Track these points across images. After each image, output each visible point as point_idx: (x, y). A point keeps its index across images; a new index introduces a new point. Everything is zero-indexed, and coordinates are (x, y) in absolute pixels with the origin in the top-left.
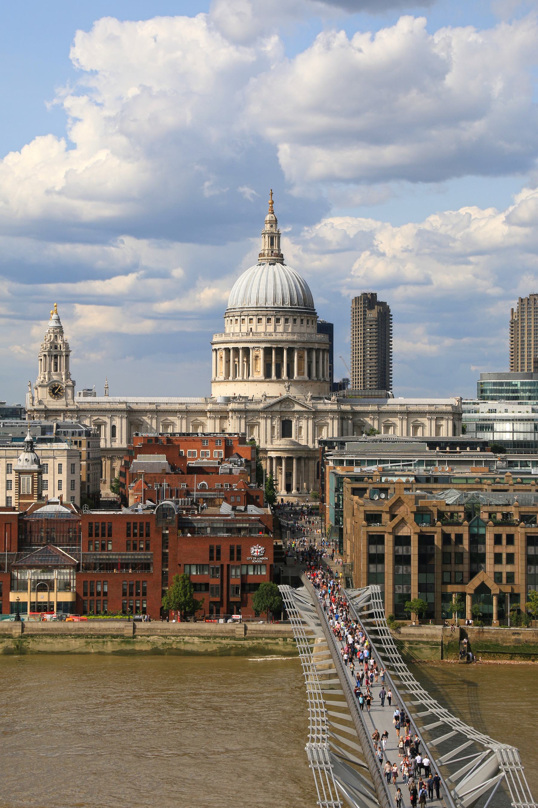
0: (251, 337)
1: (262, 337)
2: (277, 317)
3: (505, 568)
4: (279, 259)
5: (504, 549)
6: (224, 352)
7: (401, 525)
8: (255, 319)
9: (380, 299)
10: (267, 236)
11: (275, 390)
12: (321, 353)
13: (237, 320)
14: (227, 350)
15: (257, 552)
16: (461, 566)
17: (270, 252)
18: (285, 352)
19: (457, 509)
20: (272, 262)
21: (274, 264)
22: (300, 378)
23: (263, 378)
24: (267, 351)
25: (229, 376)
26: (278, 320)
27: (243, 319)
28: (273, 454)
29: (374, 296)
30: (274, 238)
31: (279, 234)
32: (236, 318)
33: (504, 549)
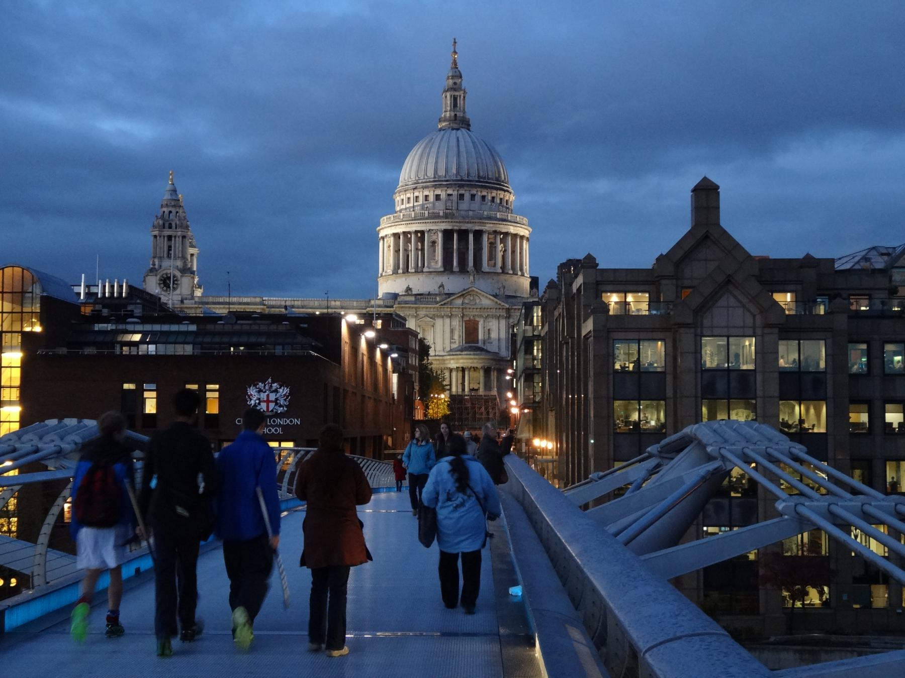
2: (460, 192)
6: (392, 238)
7: (722, 302)
10: (448, 94)
12: (518, 241)
13: (409, 198)
14: (396, 236)
15: (268, 401)
17: (453, 114)
18: (471, 237)
20: (455, 126)
21: (458, 129)
23: (442, 269)
25: (399, 268)
27: (417, 197)
31: (465, 92)
32: (408, 195)
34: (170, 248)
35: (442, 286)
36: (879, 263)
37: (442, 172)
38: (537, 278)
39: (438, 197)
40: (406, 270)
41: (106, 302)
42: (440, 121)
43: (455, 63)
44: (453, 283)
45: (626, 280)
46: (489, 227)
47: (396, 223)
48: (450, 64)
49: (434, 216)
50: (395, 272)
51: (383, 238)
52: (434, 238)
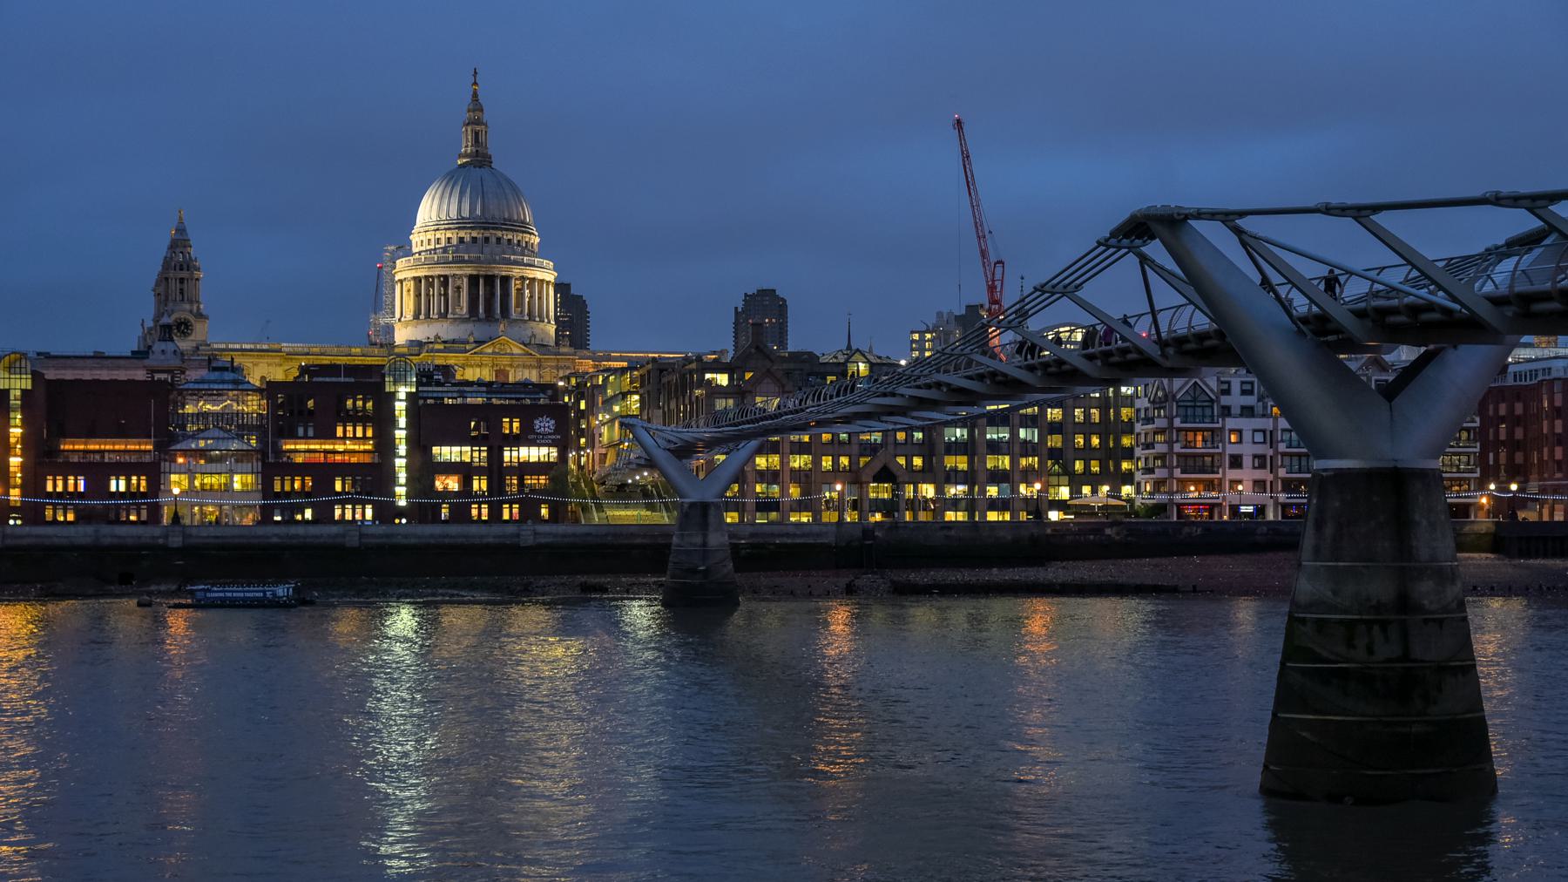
9: (573, 291)
14: (417, 280)
24: (474, 280)
29: (568, 286)
36: (841, 359)
37: (466, 214)
39: (461, 240)
40: (428, 316)
42: (461, 156)
43: (475, 94)
44: (479, 330)
45: (718, 367)
46: (516, 272)
47: (415, 267)
48: (469, 98)
49: (458, 261)
50: (416, 316)
51: (401, 281)
52: (458, 283)
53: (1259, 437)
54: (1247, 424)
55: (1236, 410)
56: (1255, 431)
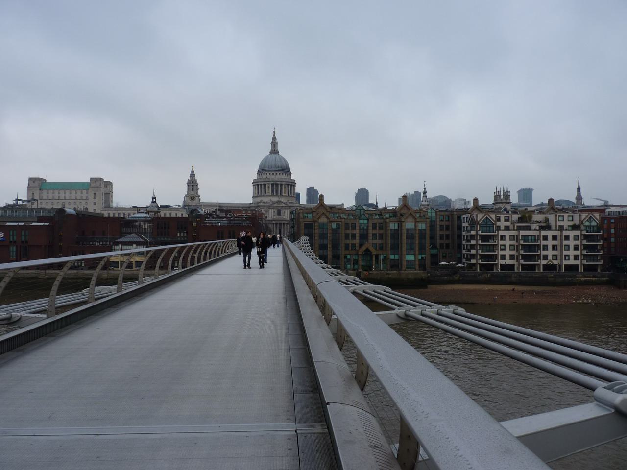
0: (267, 180)
1: (271, 180)
3: (378, 242)
4: (277, 153)
5: (377, 231)
8: (268, 174)
9: (315, 189)
11: (275, 199)
14: (258, 185)
16: (354, 241)
19: (352, 212)
22: (285, 195)
24: (273, 185)
26: (276, 174)
28: (274, 222)
29: (313, 187)
30: (274, 144)
33: (377, 231)
34: (192, 188)
35: (271, 200)
38: (299, 194)
41: (208, 214)
53: (512, 238)
54: (507, 234)
55: (502, 227)
56: (510, 236)
